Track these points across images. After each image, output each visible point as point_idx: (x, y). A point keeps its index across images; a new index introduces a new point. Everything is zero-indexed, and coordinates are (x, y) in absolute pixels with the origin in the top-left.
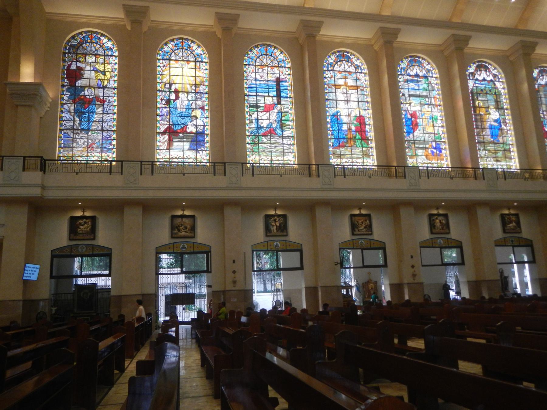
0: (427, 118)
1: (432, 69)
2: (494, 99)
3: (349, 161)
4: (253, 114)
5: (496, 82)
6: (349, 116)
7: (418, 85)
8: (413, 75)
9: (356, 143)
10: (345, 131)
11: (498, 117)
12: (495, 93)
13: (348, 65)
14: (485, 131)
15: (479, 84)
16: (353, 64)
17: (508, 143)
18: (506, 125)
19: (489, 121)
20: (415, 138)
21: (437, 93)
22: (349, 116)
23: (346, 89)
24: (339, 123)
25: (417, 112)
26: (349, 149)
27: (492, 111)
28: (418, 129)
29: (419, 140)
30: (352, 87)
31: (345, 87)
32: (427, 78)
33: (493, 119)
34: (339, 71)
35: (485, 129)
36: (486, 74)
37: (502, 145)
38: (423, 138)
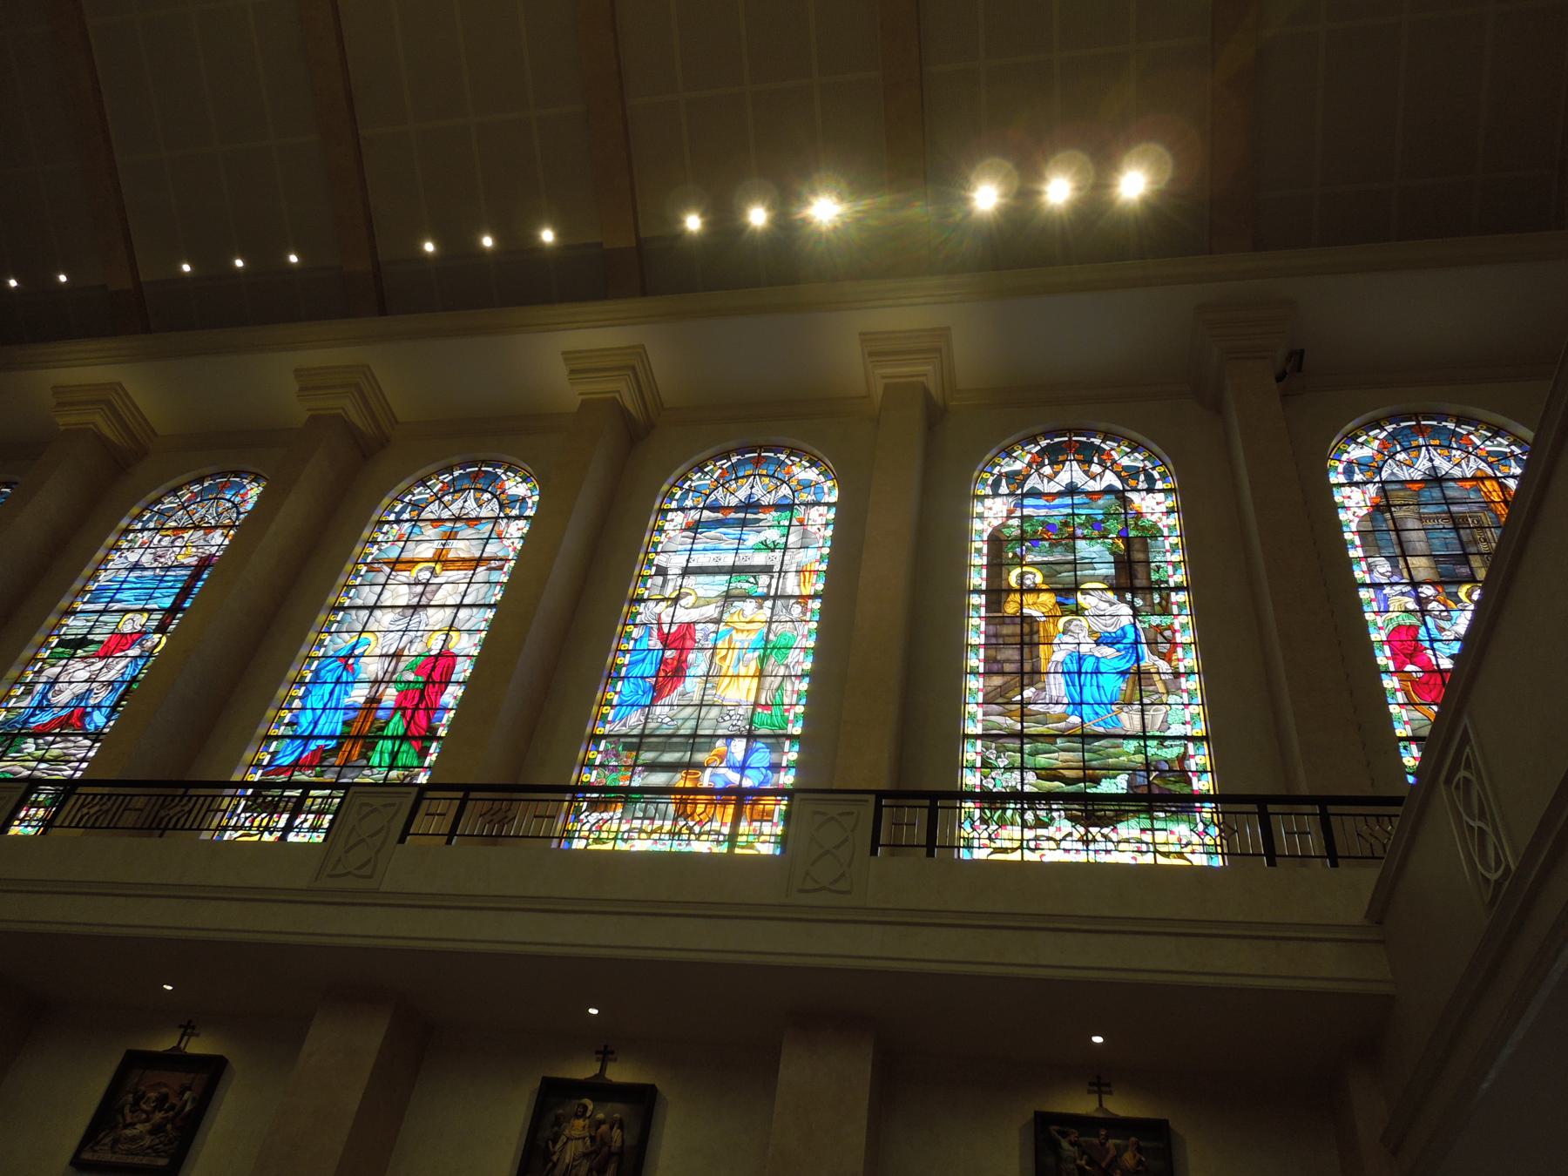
2: (1113, 553)
9: (370, 753)
14: (1040, 685)
15: (1049, 508)
20: (652, 725)
22: (397, 655)
23: (433, 571)
29: (670, 732)
33: (1092, 632)
35: (1036, 677)
36: (1086, 472)
38: (692, 723)
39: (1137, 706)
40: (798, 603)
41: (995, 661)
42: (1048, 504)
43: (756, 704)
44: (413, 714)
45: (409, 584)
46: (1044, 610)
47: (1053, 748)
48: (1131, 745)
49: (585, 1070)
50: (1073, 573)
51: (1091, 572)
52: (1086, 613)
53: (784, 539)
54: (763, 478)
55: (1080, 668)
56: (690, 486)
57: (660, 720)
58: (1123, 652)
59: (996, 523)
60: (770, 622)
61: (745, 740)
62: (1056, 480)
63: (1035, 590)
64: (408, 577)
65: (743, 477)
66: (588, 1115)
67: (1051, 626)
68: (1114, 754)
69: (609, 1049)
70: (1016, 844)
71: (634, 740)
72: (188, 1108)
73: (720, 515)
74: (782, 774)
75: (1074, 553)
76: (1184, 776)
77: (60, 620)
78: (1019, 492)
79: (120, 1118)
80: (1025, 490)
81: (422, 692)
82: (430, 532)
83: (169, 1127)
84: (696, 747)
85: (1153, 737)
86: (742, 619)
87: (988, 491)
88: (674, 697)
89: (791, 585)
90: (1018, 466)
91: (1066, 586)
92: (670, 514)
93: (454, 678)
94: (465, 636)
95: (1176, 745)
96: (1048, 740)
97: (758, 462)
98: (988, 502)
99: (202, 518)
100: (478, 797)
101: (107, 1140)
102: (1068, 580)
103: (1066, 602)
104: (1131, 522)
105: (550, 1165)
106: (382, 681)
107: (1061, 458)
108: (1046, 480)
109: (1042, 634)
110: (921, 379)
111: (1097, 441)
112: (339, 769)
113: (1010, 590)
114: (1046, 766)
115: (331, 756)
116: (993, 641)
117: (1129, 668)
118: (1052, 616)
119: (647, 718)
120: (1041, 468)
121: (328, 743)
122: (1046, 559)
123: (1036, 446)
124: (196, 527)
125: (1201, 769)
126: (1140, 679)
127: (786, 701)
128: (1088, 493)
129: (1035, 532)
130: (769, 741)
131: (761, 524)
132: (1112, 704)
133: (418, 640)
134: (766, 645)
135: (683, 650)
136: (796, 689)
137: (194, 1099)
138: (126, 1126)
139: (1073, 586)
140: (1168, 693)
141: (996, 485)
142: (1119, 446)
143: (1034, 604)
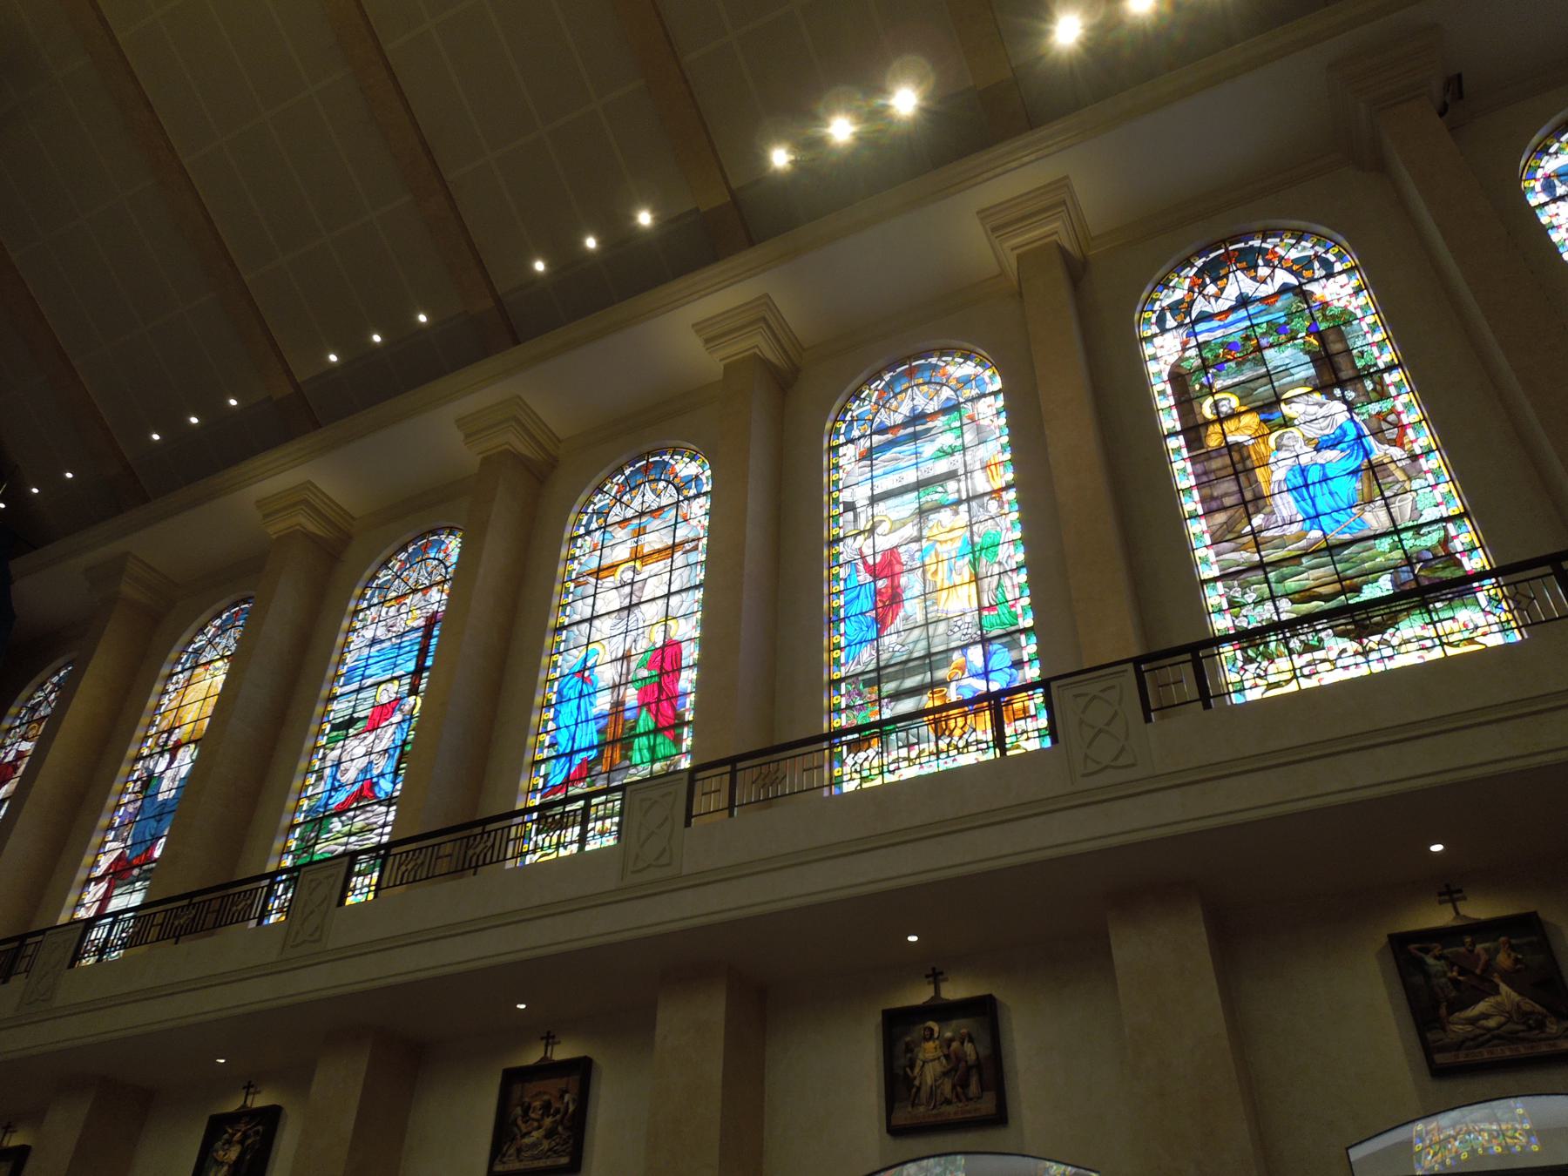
2: (1307, 353)
4: (333, 749)
9: (630, 753)
14: (1267, 510)
15: (1225, 326)
20: (884, 656)
22: (626, 657)
23: (634, 570)
29: (904, 658)
33: (1308, 441)
35: (1261, 502)
36: (1254, 279)
38: (923, 644)
39: (1379, 502)
40: (992, 499)
41: (1213, 498)
42: (1222, 323)
43: (981, 609)
44: (657, 706)
45: (616, 588)
46: (1250, 432)
47: (1300, 569)
48: (1384, 544)
49: (920, 995)
50: (1270, 386)
51: (1289, 379)
52: (1296, 422)
53: (960, 441)
54: (921, 388)
55: (1305, 479)
56: (852, 416)
57: (891, 650)
58: (1349, 451)
59: (1173, 359)
60: (971, 525)
61: (980, 647)
62: (1223, 296)
63: (1235, 415)
64: (614, 582)
65: (901, 392)
66: (936, 1035)
67: (1262, 446)
68: (1369, 557)
69: (937, 971)
70: (1288, 676)
71: (872, 675)
72: (571, 1108)
73: (889, 436)
74: (1027, 668)
75: (1265, 364)
76: (1451, 559)
77: (326, 707)
78: (1188, 320)
79: (516, 1130)
80: (1193, 318)
81: (659, 684)
82: (620, 534)
83: (560, 1128)
84: (934, 665)
85: (1407, 529)
87: (1155, 330)
88: (899, 623)
89: (981, 483)
90: (1179, 294)
91: (1266, 402)
92: (841, 449)
93: (684, 663)
94: (682, 621)
95: (1434, 531)
96: (1292, 562)
97: (911, 373)
98: (1158, 341)
99: (417, 582)
100: (1531, 576)
101: (512, 1151)
102: (1266, 394)
103: (1271, 417)
104: (1318, 315)
105: (914, 1090)
106: (620, 685)
107: (1222, 272)
108: (1212, 300)
109: (1254, 457)
110: (1055, 237)
111: (1256, 243)
112: (606, 775)
113: (1208, 423)
114: (1298, 589)
115: (597, 765)
116: (1205, 479)
117: (1360, 466)
118: (1260, 436)
119: (878, 651)
120: (1204, 288)
121: (590, 753)
122: (1236, 380)
123: (1192, 268)
124: (414, 591)
125: (1469, 547)
126: (1374, 473)
127: (1010, 597)
128: (1262, 300)
129: (1217, 356)
130: (1004, 640)
131: (932, 432)
132: (1351, 507)
133: (641, 637)
134: (973, 548)
135: (893, 576)
136: (1015, 583)
137: (574, 1100)
138: (524, 1136)
139: (1274, 399)
140: (1410, 479)
141: (1161, 321)
142: (1282, 240)
143: (1237, 429)
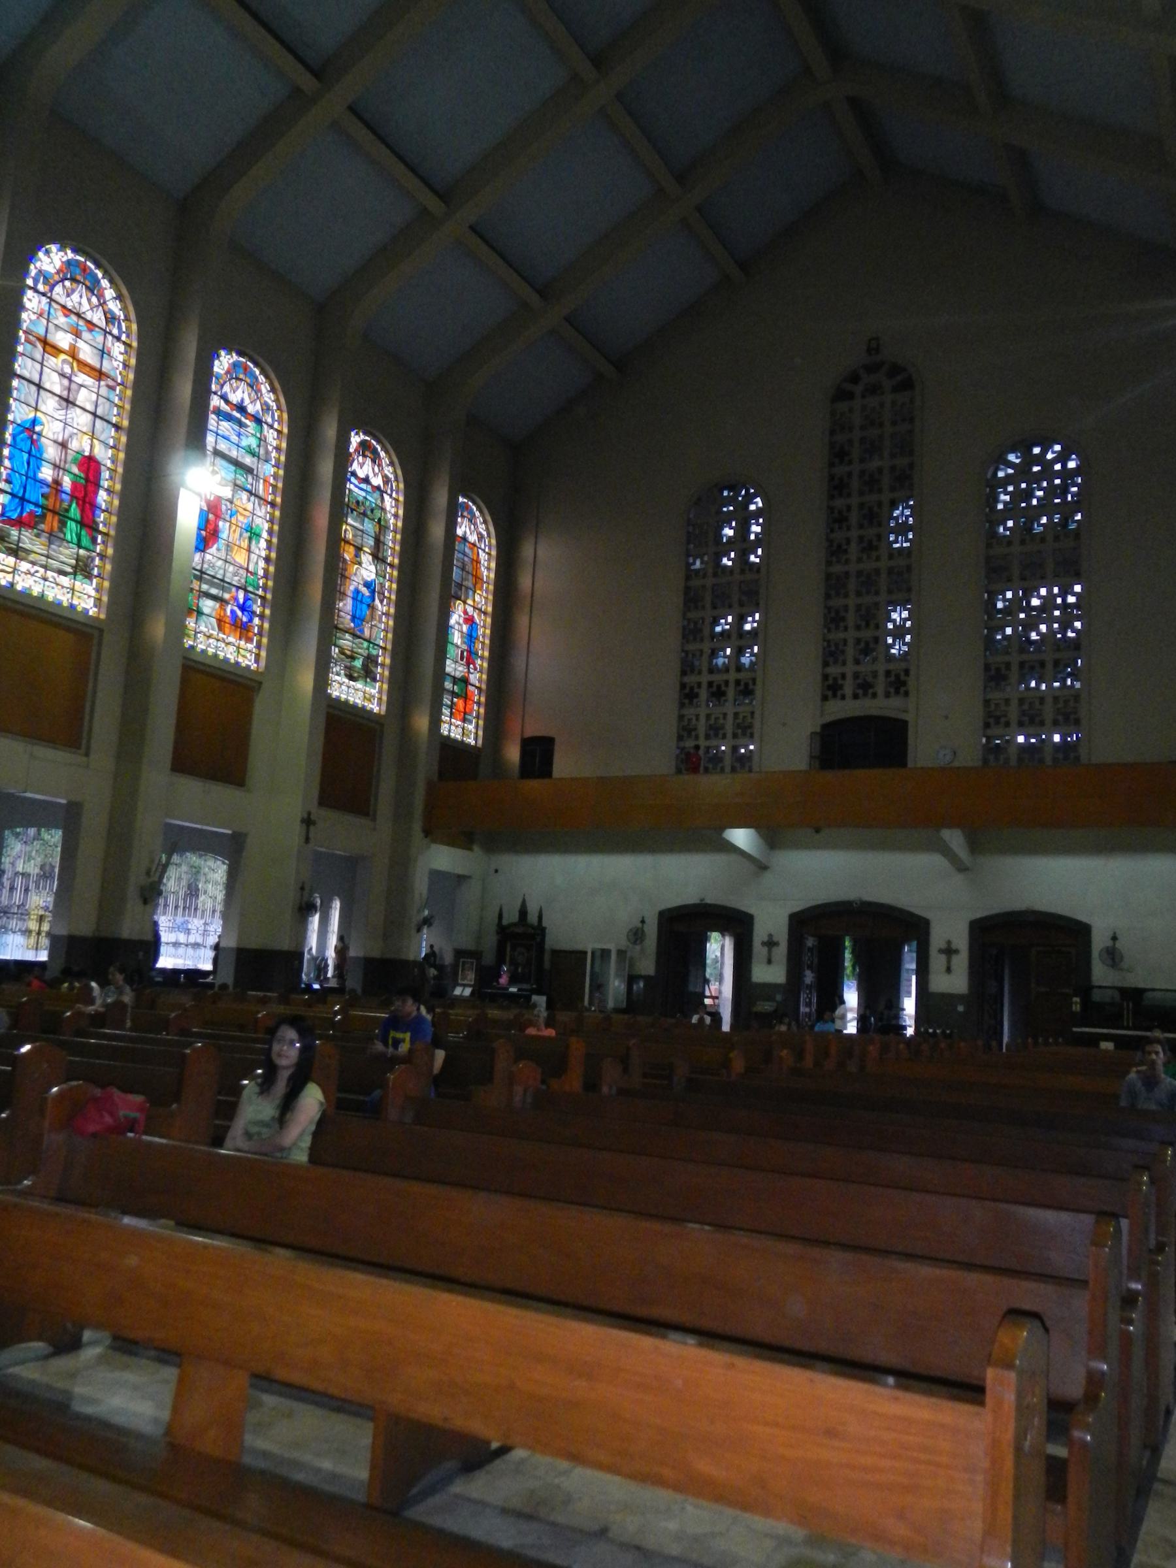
0: (240, 525)
1: (275, 408)
2: (375, 532)
3: (37, 572)
5: (385, 495)
6: (64, 445)
7: (239, 435)
8: (235, 402)
9: (64, 529)
10: (43, 482)
11: (373, 576)
12: (380, 520)
13: (89, 300)
14: (345, 602)
15: (356, 486)
16: (102, 304)
17: (376, 643)
18: (382, 602)
19: (356, 579)
20: (205, 566)
21: (273, 470)
22: (64, 445)
24: (35, 456)
25: (223, 502)
26: (44, 539)
27: (366, 558)
28: (215, 546)
29: (212, 573)
30: (88, 369)
31: (70, 359)
32: (262, 426)
33: (363, 579)
34: (64, 307)
36: (373, 469)
37: (365, 644)
38: (221, 572)
81: (85, 487)
86: (241, 506)
119: (203, 560)
121: (36, 509)
